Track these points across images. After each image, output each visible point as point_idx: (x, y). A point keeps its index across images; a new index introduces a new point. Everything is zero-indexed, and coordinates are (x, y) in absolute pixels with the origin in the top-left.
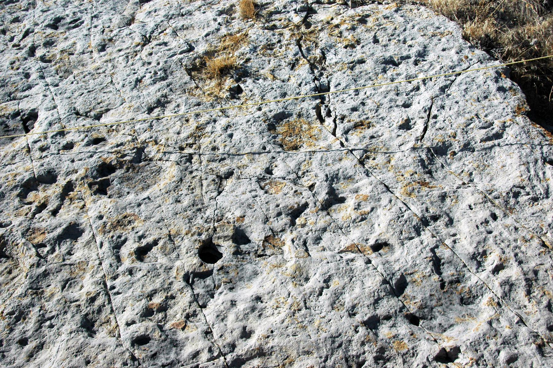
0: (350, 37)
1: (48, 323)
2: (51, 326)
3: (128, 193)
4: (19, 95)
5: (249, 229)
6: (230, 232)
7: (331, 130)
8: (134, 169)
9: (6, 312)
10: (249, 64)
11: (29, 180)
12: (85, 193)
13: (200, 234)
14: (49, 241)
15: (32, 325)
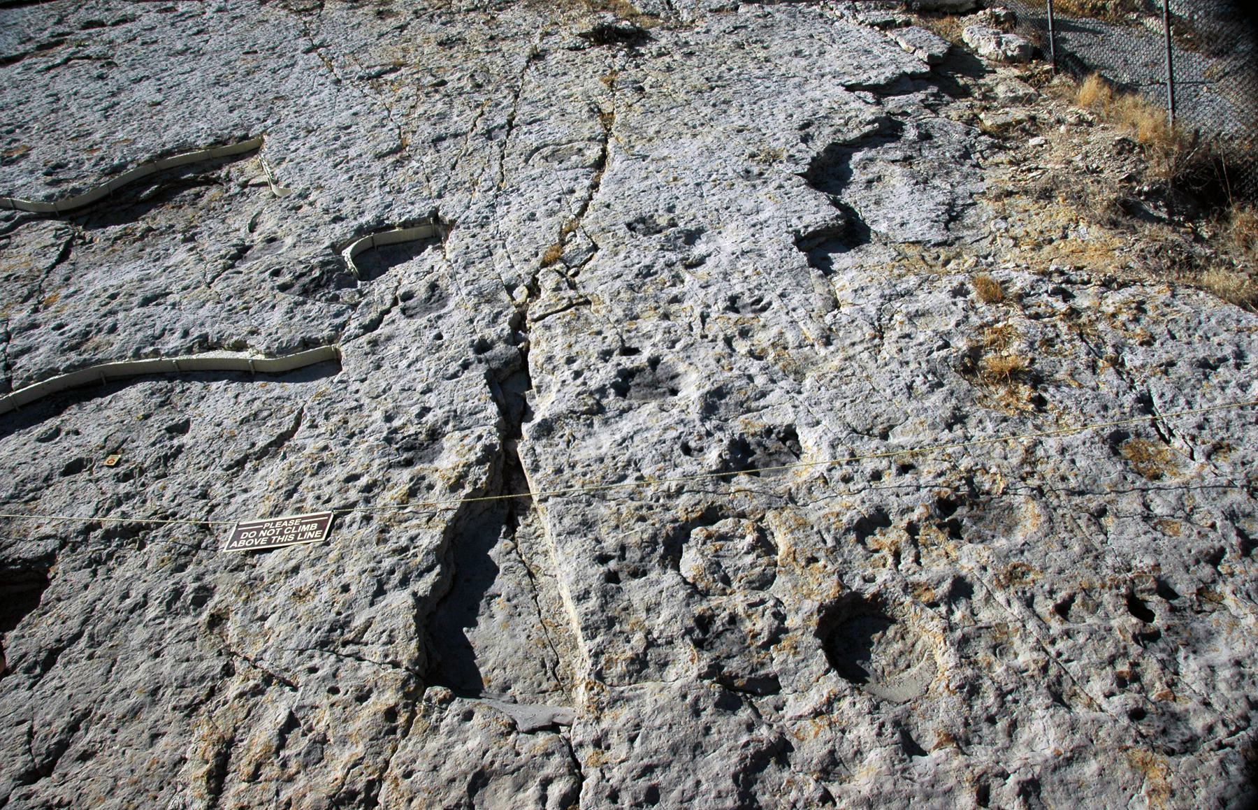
0: (1138, 331)
1: (1010, 698)
2: (1016, 701)
3: (993, 537)
4: (754, 405)
5: (1171, 581)
6: (1150, 584)
7: (1188, 453)
8: (978, 505)
9: (952, 686)
10: (1037, 366)
11: (859, 522)
12: (937, 537)
13: (1118, 588)
14: (941, 599)
15: (992, 700)
